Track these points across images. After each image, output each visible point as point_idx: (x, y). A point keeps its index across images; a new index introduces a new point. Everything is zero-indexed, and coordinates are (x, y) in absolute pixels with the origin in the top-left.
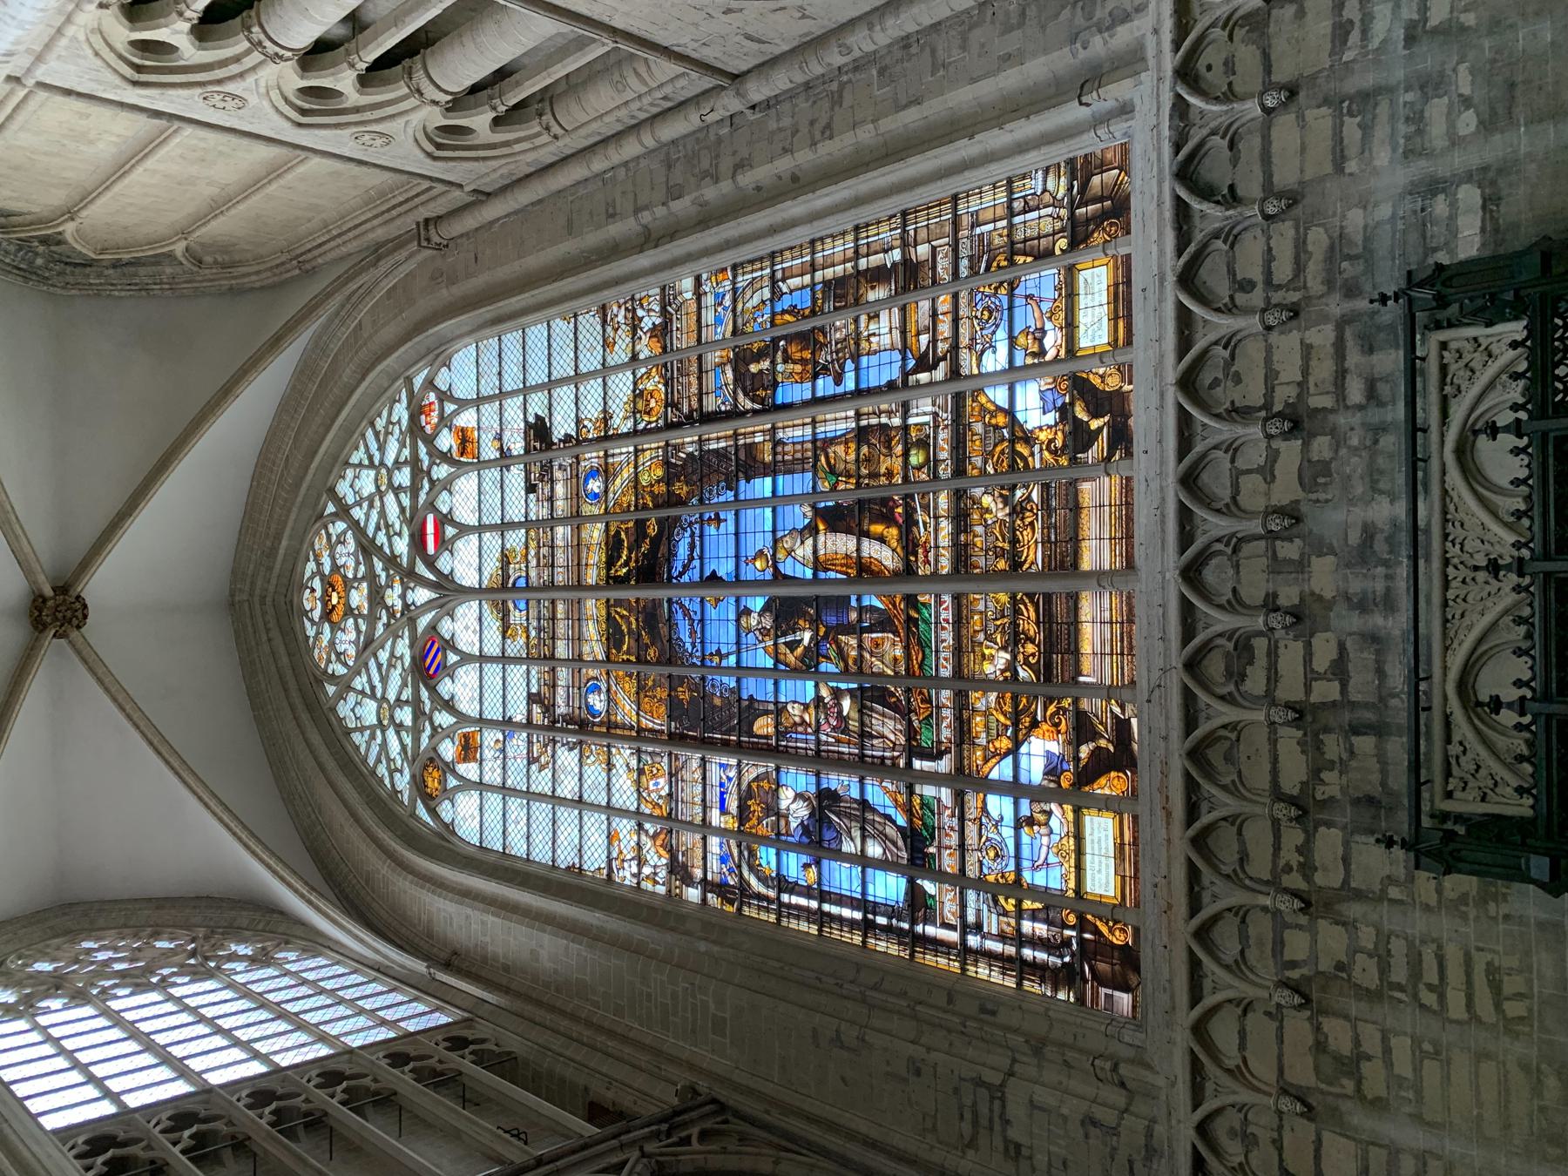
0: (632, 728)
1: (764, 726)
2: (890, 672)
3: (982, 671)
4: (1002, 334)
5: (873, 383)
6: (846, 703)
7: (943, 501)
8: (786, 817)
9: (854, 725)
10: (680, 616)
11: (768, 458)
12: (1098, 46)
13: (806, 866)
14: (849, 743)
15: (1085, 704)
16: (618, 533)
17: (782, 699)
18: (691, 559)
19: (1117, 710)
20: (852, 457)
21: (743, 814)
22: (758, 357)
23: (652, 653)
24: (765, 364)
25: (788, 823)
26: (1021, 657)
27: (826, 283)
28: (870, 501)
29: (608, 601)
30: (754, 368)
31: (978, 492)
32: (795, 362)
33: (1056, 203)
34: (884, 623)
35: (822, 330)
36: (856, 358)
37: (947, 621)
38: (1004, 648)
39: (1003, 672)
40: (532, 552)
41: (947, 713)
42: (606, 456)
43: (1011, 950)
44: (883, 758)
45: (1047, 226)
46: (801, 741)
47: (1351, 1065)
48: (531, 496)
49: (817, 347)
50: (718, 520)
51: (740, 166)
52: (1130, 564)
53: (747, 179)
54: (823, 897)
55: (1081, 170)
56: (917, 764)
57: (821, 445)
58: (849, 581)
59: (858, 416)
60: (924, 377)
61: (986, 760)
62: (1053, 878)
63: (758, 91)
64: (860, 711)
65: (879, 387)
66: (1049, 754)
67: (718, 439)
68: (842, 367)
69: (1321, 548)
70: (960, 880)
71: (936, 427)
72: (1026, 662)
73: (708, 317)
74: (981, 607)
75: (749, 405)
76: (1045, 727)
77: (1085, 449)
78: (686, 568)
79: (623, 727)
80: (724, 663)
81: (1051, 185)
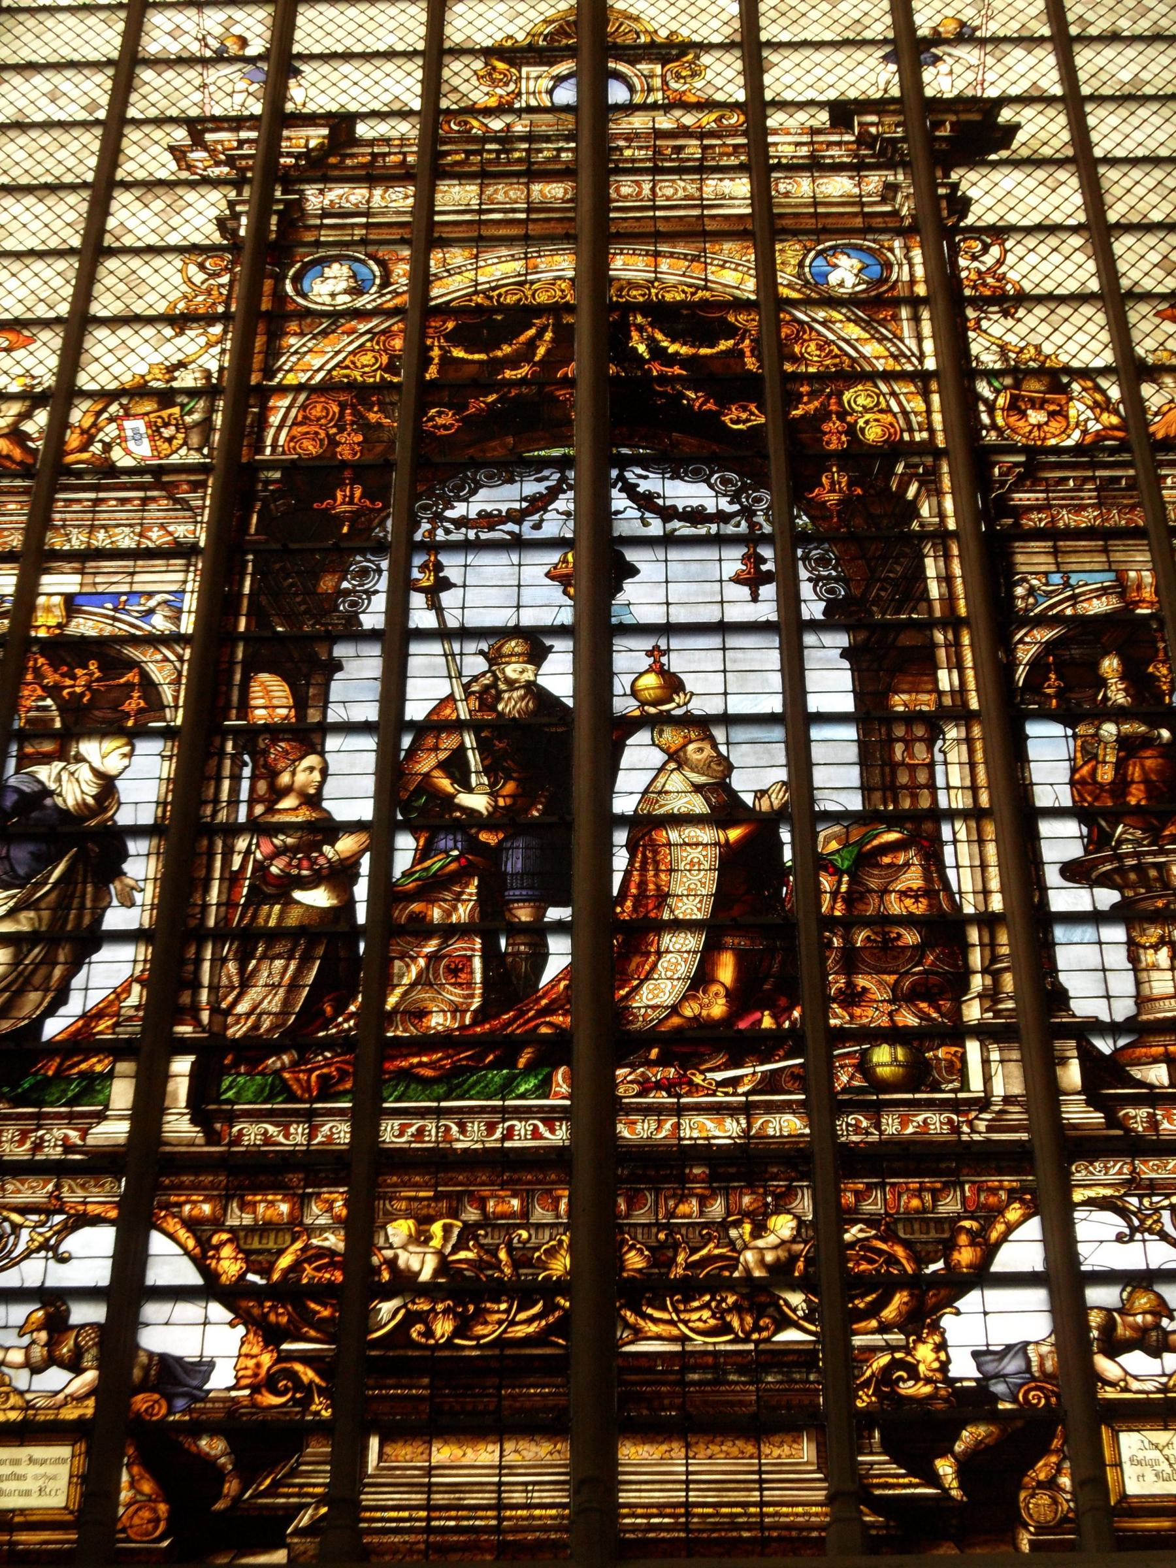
0: (269, 373)
2: (392, 1001)
3: (392, 1217)
5: (1064, 957)
6: (319, 898)
7: (790, 1125)
8: (62, 755)
9: (271, 915)
10: (532, 488)
14: (228, 904)
15: (319, 1449)
16: (731, 331)
17: (332, 743)
19: (305, 1520)
20: (895, 907)
23: (443, 419)
24: (1118, 695)
25: (46, 759)
26: (423, 1306)
28: (791, 952)
29: (569, 308)
30: (1110, 665)
31: (805, 1205)
32: (1120, 766)
37: (509, 1135)
38: (444, 1267)
39: (392, 1263)
40: (689, 120)
41: (298, 1134)
42: (915, 302)
44: (196, 985)
46: (235, 790)
48: (824, 116)
56: (182, 1065)
59: (987, 921)
60: (1072, 1074)
61: (191, 1224)
64: (300, 932)
65: (1054, 970)
66: (205, 1367)
67: (947, 579)
68: (1105, 881)
71: (955, 1106)
72: (412, 1318)
74: (540, 1214)
75: (1025, 654)
76: (267, 1359)
77: (895, 1450)
78: (646, 502)
79: (273, 352)
80: (418, 600)
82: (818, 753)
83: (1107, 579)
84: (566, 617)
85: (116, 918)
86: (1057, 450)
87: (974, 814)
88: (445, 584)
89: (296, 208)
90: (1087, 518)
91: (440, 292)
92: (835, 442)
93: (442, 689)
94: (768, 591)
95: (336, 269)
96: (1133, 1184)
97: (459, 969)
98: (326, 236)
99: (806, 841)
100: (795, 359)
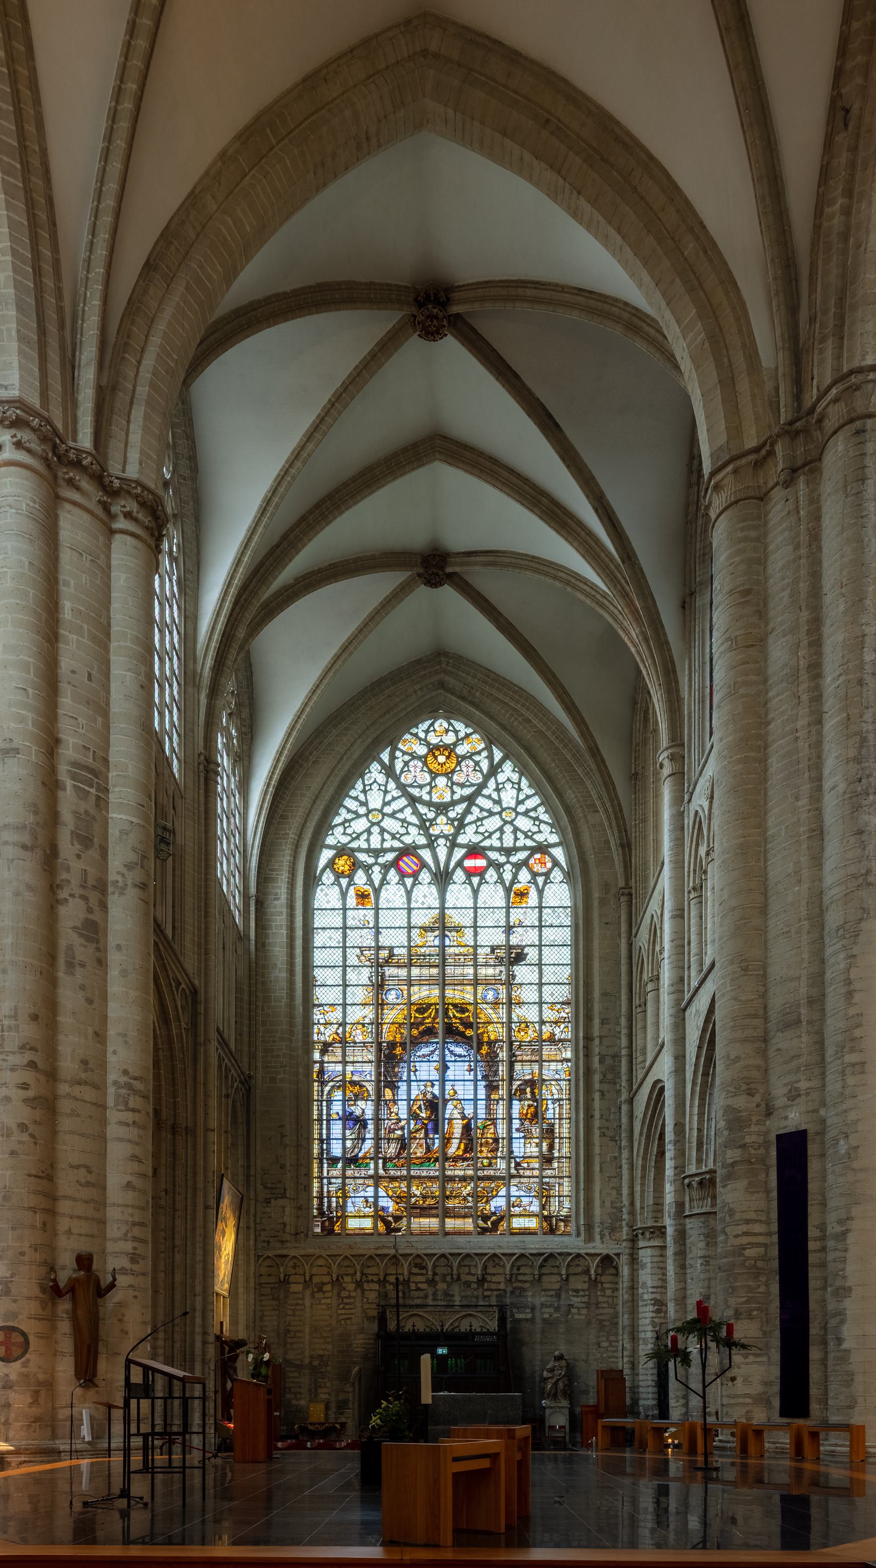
1: (388, 1094)
4: (522, 1193)
7: (470, 1172)
9: (392, 1136)
11: (492, 1097)
16: (468, 1011)
18: (455, 1055)
21: (353, 1083)
22: (532, 1093)
23: (415, 1032)
24: (529, 1096)
27: (553, 1125)
30: (528, 1090)
31: (472, 1185)
34: (428, 1149)
36: (525, 1137)
40: (462, 950)
45: (552, 1209)
47: (320, 1290)
49: (531, 1120)
50: (470, 1070)
52: (447, 1234)
54: (328, 1121)
56: (380, 1161)
57: (494, 1121)
60: (513, 1165)
62: (350, 1209)
69: (449, 1285)
70: (344, 1177)
73: (553, 1066)
75: (514, 1087)
78: (451, 1052)
79: (382, 1014)
85: (368, 1136)
89: (383, 974)
90: (528, 1058)
91: (414, 998)
92: (486, 1039)
93: (417, 1092)
95: (393, 992)
98: (391, 983)
99: (476, 1123)
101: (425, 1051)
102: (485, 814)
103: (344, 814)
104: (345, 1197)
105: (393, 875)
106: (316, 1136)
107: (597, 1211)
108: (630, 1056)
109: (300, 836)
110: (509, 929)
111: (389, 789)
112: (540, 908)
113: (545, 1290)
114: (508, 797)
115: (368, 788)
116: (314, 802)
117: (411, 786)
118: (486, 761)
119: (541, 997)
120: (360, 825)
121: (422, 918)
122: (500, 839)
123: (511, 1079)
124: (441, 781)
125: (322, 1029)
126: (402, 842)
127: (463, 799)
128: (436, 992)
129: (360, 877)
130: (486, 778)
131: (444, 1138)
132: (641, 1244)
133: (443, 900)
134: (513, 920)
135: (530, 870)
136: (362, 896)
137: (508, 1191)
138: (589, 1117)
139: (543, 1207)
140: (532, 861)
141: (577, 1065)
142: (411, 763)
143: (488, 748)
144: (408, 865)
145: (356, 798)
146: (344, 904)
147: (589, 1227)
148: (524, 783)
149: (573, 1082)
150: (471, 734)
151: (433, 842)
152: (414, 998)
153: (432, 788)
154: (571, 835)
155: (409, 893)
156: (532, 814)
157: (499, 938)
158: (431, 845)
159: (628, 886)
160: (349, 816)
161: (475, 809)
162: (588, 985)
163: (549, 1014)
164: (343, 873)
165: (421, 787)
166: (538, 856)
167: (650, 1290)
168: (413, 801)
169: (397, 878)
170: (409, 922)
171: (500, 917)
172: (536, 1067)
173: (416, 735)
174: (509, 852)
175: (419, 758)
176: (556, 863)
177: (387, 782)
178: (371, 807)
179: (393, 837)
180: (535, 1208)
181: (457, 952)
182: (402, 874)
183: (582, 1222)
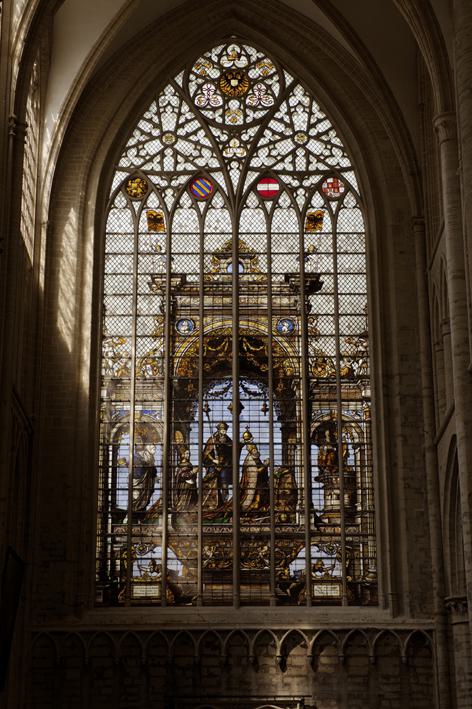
4: (324, 555)
5: (314, 497)
6: (190, 482)
7: (267, 529)
8: (144, 449)
10: (225, 386)
11: (290, 440)
12: (406, 600)
13: (125, 460)
14: (175, 483)
16: (262, 344)
18: (250, 393)
20: (287, 486)
22: (332, 436)
24: (328, 440)
25: (141, 450)
27: (356, 472)
30: (327, 433)
32: (327, 456)
33: (364, 578)
35: (337, 471)
42: (299, 336)
43: (109, 556)
45: (357, 573)
51: (405, 439)
53: (399, 441)
55: (373, 587)
58: (238, 484)
59: (302, 489)
60: (313, 521)
62: (136, 573)
63: (428, 456)
67: (300, 411)
68: (321, 481)
71: (294, 526)
72: (209, 564)
73: (352, 406)
75: (312, 430)
77: (281, 588)
79: (174, 347)
80: (204, 414)
81: (371, 575)
82: (275, 452)
83: (328, 412)
84: (231, 419)
85: (157, 486)
86: (322, 378)
87: (301, 466)
88: (209, 410)
89: (175, 303)
90: (325, 397)
93: (209, 435)
94: (267, 413)
95: (185, 323)
96: (320, 541)
97: (214, 498)
100: (275, 352)
101: (218, 388)
102: (277, 137)
103: (137, 136)
104: (132, 559)
105: (186, 199)
106: (101, 486)
107: (405, 577)
108: (432, 397)
109: (93, 160)
110: (304, 256)
111: (183, 111)
112: (335, 234)
113: (352, 676)
114: (300, 121)
115: (162, 110)
116: (109, 125)
117: (204, 108)
118: (277, 85)
119: (337, 329)
120: (154, 147)
121: (214, 244)
122: (293, 163)
123: (309, 420)
124: (234, 104)
125: (110, 363)
126: (195, 165)
127: (255, 122)
128: (230, 323)
129: (153, 201)
130: (278, 102)
131: (238, 488)
132: (455, 619)
133: (236, 225)
134: (306, 245)
135: (323, 194)
136: (154, 221)
137: (309, 551)
138: (392, 466)
139: (347, 571)
140: (325, 186)
141: (377, 405)
142: (205, 87)
143: (280, 73)
144: (201, 187)
145: (150, 121)
146: (137, 228)
147: (397, 595)
148: (315, 107)
149: (374, 424)
150: (263, 58)
151: (226, 165)
152: (207, 329)
153: (224, 111)
154: (362, 161)
155: (202, 217)
156: (324, 138)
157: (291, 265)
158: (224, 168)
159: (420, 216)
160: (142, 139)
161: (267, 133)
162: (385, 318)
163: (347, 348)
164: (135, 195)
165: (214, 109)
166: (330, 180)
167: (468, 677)
168: (207, 123)
169: (190, 201)
170: (202, 248)
171: (294, 242)
172: (335, 407)
173: (210, 59)
174: (301, 176)
175: (212, 81)
176: (349, 188)
177: (181, 105)
178: (165, 129)
179: (187, 160)
180: (337, 573)
181: (251, 280)
182: (196, 199)
183: (390, 591)
